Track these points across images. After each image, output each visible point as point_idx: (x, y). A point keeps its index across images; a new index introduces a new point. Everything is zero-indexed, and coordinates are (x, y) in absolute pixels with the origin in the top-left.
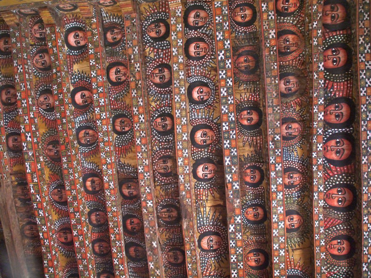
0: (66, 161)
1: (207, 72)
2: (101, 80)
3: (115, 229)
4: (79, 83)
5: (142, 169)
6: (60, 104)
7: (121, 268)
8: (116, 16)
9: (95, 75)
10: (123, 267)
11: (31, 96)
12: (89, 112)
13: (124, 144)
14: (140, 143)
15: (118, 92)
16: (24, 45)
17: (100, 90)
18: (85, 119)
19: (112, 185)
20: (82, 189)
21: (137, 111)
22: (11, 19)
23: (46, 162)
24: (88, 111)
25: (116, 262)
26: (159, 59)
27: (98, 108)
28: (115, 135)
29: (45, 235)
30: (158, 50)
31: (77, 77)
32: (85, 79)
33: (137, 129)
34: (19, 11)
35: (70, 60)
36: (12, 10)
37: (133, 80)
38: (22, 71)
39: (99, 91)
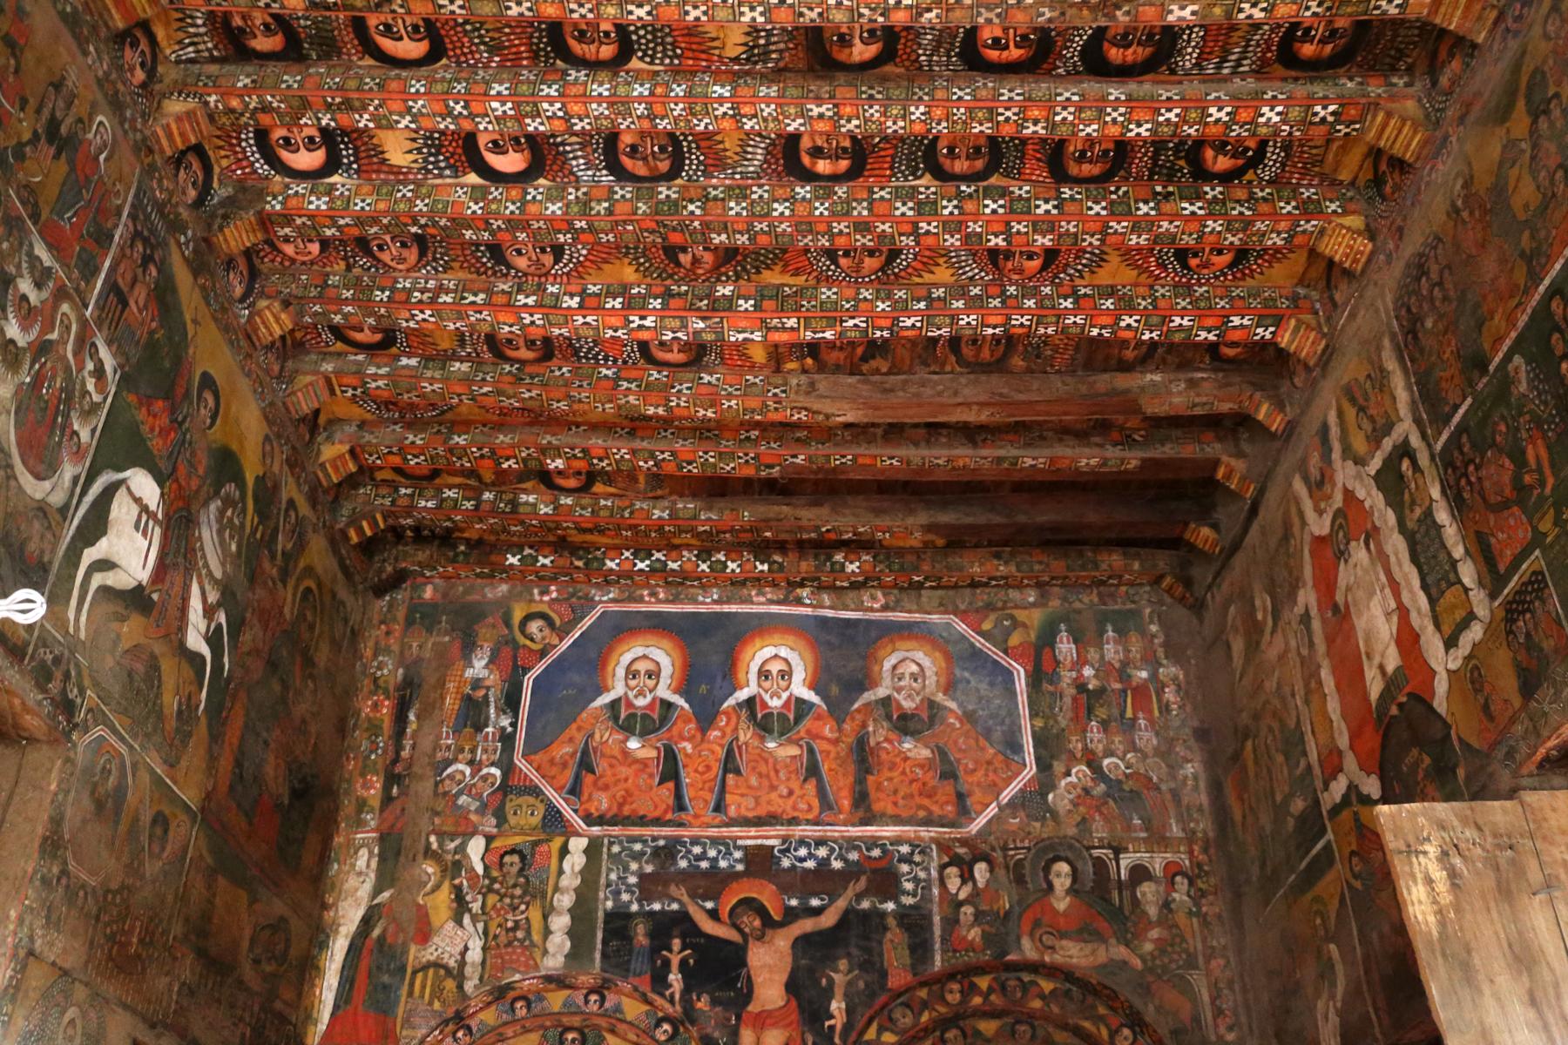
0: (724, 237)
2: (421, 102)
3: (1001, 118)
4: (453, 154)
5: (752, 9)
7: (1171, 115)
10: (1169, 110)
11: (510, 293)
13: (669, 40)
14: (647, 8)
16: (348, 294)
17: (458, 108)
19: (823, 109)
20: (841, 191)
23: (738, 277)
25: (1143, 131)
27: (528, 121)
28: (635, 63)
29: (993, 320)
33: (591, 11)
34: (242, 300)
35: (378, 172)
36: (243, 321)
38: (428, 312)
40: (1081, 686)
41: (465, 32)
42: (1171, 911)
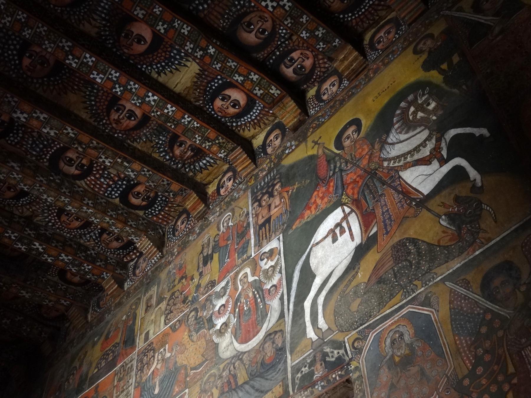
1: (34, 208)
6: (150, 15)
8: (208, 167)
9: (147, 99)
12: (105, 26)
15: (100, 94)
18: (98, 10)
21: (38, 118)
22: (346, 63)
24: (108, 27)
26: (100, 174)
27: (91, 64)
30: (113, 181)
31: (178, 57)
32: (163, 64)
37: (92, 143)
39: (117, 86)
41: (96, 98)
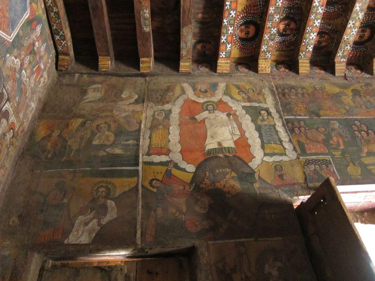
40: (34, 45)
42: (4, 138)
